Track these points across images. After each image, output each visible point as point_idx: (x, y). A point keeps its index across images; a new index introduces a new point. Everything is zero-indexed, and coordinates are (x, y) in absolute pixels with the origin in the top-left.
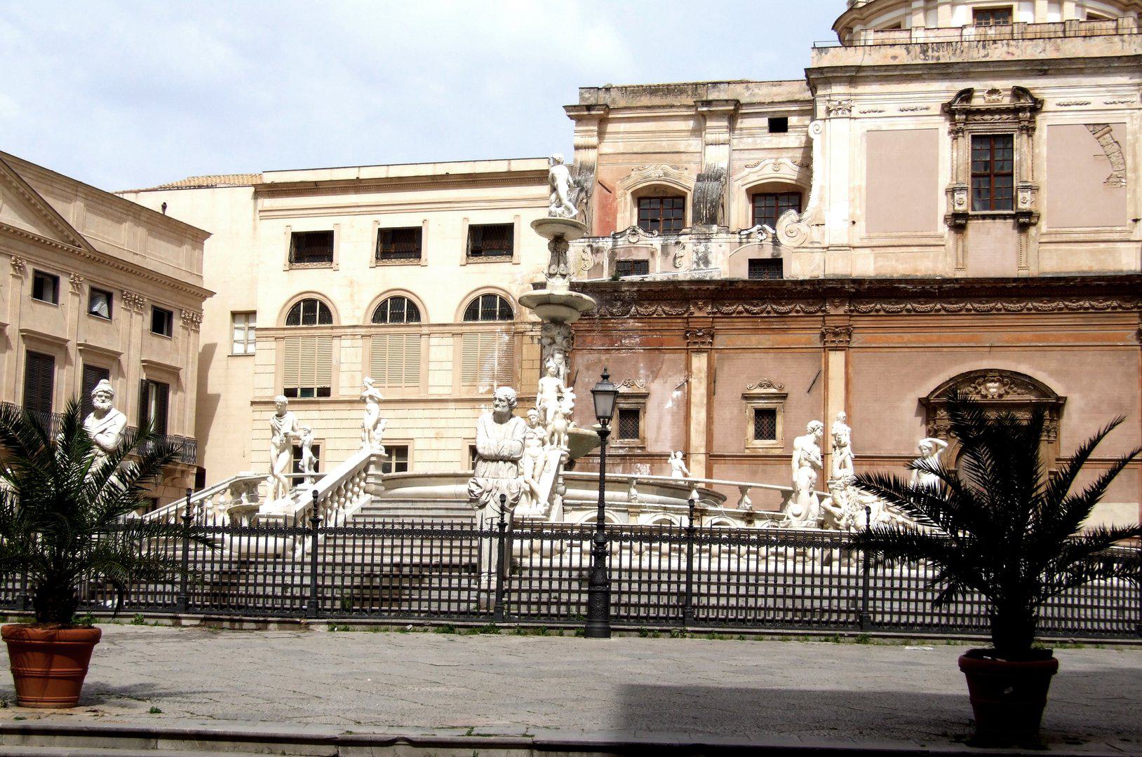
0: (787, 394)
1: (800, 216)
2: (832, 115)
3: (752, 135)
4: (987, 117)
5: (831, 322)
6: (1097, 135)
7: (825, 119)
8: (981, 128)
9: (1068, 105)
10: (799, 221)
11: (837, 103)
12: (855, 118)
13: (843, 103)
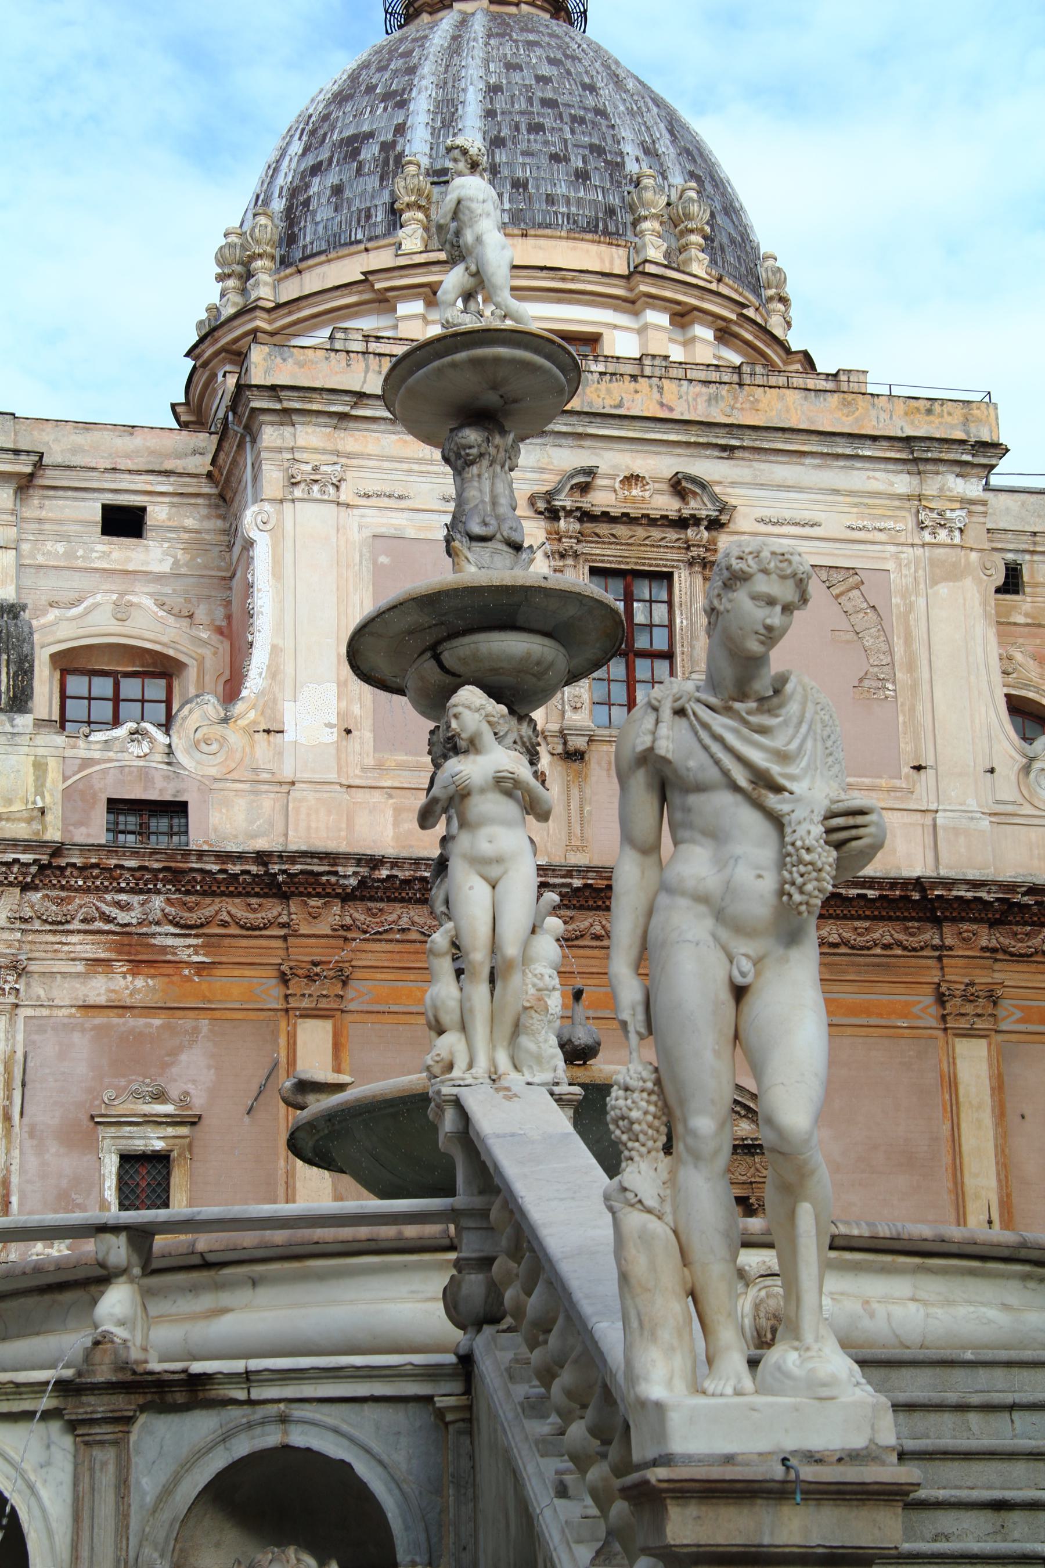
0: (200, 1117)
1: (226, 710)
2: (298, 493)
3: (65, 537)
4: (621, 530)
5: (302, 953)
6: (835, 591)
7: (281, 501)
8: (608, 555)
9: (777, 523)
10: (225, 720)
11: (308, 468)
12: (348, 506)
13: (323, 468)
